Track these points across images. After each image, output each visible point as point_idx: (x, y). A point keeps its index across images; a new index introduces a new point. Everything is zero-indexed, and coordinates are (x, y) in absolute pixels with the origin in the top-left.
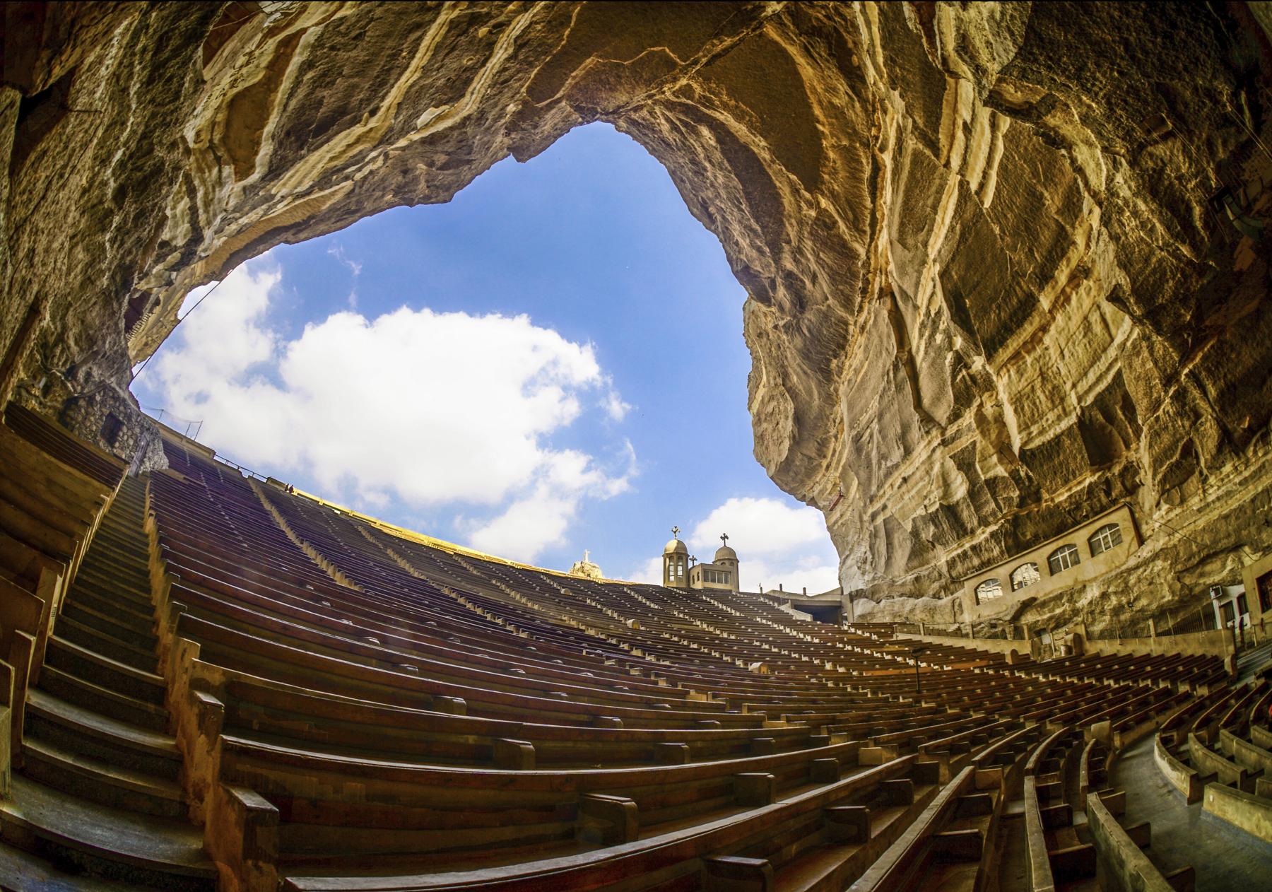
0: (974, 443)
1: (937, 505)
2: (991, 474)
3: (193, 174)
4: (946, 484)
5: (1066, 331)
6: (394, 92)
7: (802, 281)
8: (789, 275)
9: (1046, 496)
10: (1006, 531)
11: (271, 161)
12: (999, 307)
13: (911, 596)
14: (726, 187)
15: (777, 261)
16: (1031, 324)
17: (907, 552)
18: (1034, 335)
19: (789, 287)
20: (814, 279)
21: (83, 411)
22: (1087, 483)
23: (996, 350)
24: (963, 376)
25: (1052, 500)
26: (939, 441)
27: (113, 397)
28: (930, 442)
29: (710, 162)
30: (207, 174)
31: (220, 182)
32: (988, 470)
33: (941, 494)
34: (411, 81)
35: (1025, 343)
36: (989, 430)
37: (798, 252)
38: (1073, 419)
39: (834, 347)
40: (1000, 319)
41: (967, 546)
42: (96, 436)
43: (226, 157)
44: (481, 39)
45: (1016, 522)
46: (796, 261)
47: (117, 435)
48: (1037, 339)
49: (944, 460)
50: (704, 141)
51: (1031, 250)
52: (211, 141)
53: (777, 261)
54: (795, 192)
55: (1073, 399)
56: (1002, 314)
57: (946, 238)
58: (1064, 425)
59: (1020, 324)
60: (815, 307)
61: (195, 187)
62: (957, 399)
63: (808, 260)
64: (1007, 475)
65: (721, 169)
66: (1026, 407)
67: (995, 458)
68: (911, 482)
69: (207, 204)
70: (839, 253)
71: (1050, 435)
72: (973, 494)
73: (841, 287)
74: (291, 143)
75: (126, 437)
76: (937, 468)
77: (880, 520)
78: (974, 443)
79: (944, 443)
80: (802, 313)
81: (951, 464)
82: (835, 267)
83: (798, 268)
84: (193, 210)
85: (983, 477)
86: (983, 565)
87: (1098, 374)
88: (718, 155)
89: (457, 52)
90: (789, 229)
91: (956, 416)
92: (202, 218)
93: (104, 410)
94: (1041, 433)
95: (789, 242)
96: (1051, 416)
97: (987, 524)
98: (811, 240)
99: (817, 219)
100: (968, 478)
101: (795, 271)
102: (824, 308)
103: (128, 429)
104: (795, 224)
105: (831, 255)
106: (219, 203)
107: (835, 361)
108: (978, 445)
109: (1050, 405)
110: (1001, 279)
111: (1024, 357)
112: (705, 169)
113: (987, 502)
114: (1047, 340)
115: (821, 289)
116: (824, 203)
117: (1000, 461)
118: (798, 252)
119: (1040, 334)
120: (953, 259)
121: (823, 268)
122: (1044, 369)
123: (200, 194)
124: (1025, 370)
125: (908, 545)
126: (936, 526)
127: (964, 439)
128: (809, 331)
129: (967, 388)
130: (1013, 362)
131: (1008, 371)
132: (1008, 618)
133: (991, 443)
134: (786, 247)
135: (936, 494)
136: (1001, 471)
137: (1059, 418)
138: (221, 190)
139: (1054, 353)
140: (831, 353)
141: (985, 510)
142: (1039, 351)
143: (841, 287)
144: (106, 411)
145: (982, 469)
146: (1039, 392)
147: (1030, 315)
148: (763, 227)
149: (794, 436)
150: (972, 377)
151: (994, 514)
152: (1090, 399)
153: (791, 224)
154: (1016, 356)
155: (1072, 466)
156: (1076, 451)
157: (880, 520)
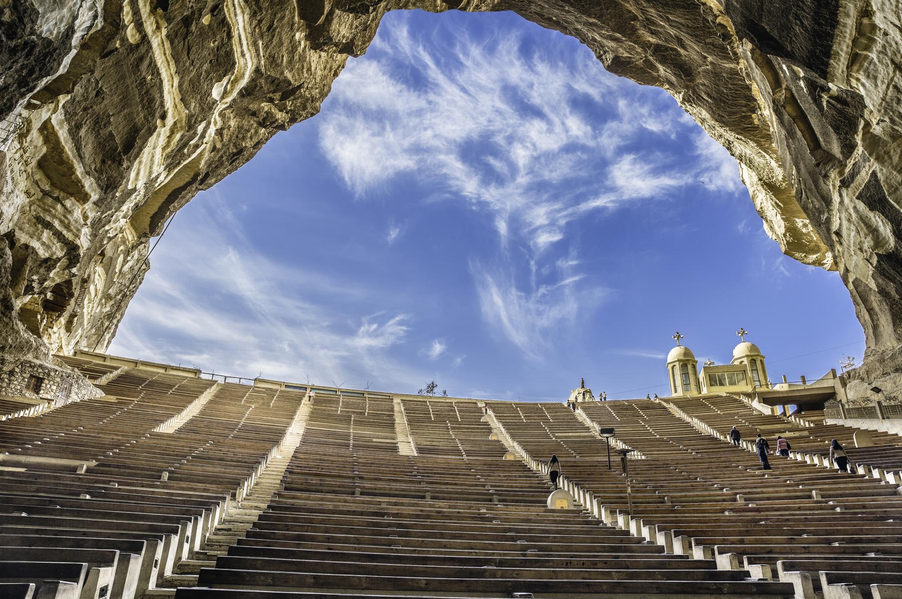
0: (874, 174)
3: (42, 215)
4: (873, 231)
6: (167, 96)
7: (673, 49)
8: (658, 50)
11: (99, 185)
12: (797, 17)
15: (638, 40)
16: (848, 15)
18: (859, 28)
19: (663, 61)
21: (6, 380)
23: (827, 65)
24: (828, 101)
26: (838, 184)
27: (31, 366)
30: (53, 211)
31: (68, 211)
33: (872, 243)
34: (176, 83)
35: (855, 41)
36: (887, 153)
37: (649, 23)
40: (806, 30)
42: (21, 391)
43: (62, 194)
44: (209, 25)
46: (653, 33)
47: (40, 386)
48: (867, 30)
52: (42, 191)
53: (638, 40)
56: (806, 22)
59: (834, 22)
60: (700, 69)
61: (49, 222)
62: (837, 129)
63: (663, 27)
68: (844, 233)
69: (67, 227)
70: (684, 7)
73: (708, 40)
74: (110, 166)
75: (48, 386)
76: (854, 215)
78: (874, 174)
80: (692, 80)
81: (861, 206)
82: (690, 24)
83: (660, 39)
84: (59, 235)
89: (194, 48)
91: (849, 148)
92: (69, 236)
93: (24, 375)
95: (635, 18)
98: (651, 7)
100: (886, 217)
103: (49, 381)
105: (679, 12)
106: (76, 222)
107: (754, 116)
108: (879, 175)
111: (866, 57)
115: (692, 51)
118: (649, 23)
119: (866, 21)
121: (679, 28)
123: (56, 224)
124: (876, 71)
125: (885, 307)
127: (863, 173)
129: (840, 112)
130: (855, 68)
131: (858, 80)
133: (895, 168)
134: (638, 25)
135: (868, 243)
138: (72, 215)
140: (744, 109)
142: (879, 39)
143: (708, 40)
144: (27, 375)
150: (837, 99)
154: (854, 59)
157: (851, 286)
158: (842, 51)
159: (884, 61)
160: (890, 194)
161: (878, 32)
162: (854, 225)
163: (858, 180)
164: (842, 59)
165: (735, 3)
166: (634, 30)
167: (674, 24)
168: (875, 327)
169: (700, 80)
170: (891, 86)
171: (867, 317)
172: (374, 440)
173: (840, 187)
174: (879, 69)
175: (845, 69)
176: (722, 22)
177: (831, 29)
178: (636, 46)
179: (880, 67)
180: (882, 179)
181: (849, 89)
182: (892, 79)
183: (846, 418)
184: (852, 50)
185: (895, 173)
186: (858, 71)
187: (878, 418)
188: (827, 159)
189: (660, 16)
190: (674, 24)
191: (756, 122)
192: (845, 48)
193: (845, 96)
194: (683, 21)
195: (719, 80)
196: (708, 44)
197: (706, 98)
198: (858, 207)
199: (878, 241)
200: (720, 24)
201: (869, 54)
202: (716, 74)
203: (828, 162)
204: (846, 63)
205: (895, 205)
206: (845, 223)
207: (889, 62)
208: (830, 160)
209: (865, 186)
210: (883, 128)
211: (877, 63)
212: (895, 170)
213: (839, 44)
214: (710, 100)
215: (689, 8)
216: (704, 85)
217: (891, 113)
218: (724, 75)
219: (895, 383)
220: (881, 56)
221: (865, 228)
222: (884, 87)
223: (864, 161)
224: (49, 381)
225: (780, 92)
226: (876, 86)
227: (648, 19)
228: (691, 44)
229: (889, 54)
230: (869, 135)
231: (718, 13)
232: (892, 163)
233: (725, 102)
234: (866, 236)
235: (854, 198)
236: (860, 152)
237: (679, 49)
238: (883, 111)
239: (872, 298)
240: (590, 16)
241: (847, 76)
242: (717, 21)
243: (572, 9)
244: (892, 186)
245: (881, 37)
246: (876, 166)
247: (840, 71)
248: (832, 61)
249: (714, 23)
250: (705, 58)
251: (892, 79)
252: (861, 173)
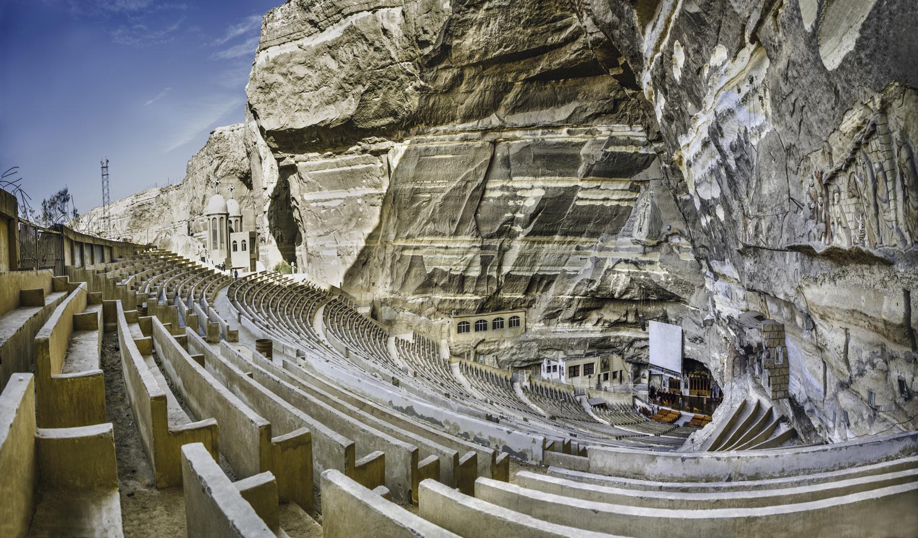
1: (459, 273)
17: (419, 283)
22: (518, 297)
38: (531, 275)
55: (537, 268)
58: (527, 274)
71: (520, 274)
79: (482, 248)
81: (478, 259)
94: (518, 271)
113: (483, 285)
114: (545, 246)
126: (450, 281)
136: (495, 274)
137: (527, 271)
146: (529, 258)
151: (483, 292)
152: (541, 273)
154: (534, 242)
155: (518, 288)
156: (523, 285)
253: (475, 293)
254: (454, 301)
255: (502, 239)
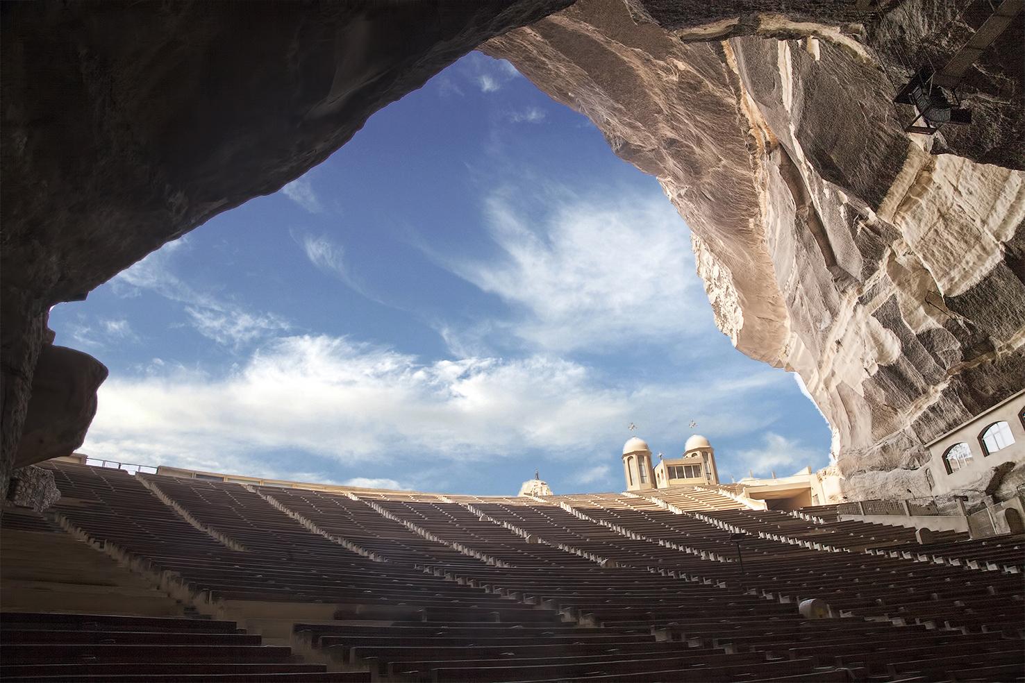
0: (894, 297)
1: (877, 368)
2: (923, 328)
4: (879, 345)
5: (952, 166)
7: (688, 146)
8: (672, 142)
9: (998, 343)
10: (959, 388)
13: (883, 469)
14: (572, 75)
17: (869, 420)
18: (918, 178)
19: (676, 156)
20: (699, 142)
23: (881, 201)
24: (863, 228)
25: (1009, 347)
26: (857, 300)
28: (849, 302)
29: (545, 56)
32: (918, 325)
33: (877, 356)
38: (998, 257)
39: (745, 207)
40: (872, 168)
41: (925, 407)
45: (966, 375)
48: (923, 181)
49: (866, 320)
50: (531, 39)
51: (878, 94)
54: (647, 62)
55: (989, 238)
56: (874, 164)
57: (793, 95)
58: (990, 264)
59: (898, 168)
60: (711, 170)
62: (864, 253)
64: (941, 326)
65: (559, 61)
66: (937, 253)
67: (922, 310)
68: (845, 343)
71: (976, 278)
72: (907, 351)
73: (729, 146)
77: (833, 388)
78: (894, 297)
79: (862, 301)
81: (875, 323)
85: (913, 332)
86: (950, 427)
87: (1008, 205)
88: (549, 49)
90: (656, 99)
91: (870, 270)
95: (660, 112)
96: (971, 257)
97: (936, 383)
99: (680, 82)
101: (678, 138)
102: (721, 170)
104: (659, 92)
105: (708, 115)
107: (751, 220)
109: (964, 246)
110: (861, 128)
111: (916, 202)
112: (544, 63)
113: (925, 358)
114: (937, 177)
115: (707, 152)
116: (682, 66)
117: (929, 312)
118: (672, 119)
119: (926, 174)
120: (804, 117)
122: (944, 210)
125: (867, 411)
127: (882, 294)
128: (713, 196)
129: (871, 239)
130: (904, 208)
132: (984, 488)
135: (872, 355)
136: (932, 323)
139: (948, 190)
140: (744, 213)
141: (927, 367)
142: (931, 190)
143: (729, 146)
145: (911, 325)
146: (946, 235)
147: (905, 157)
148: (626, 105)
149: (743, 301)
150: (872, 228)
152: (1010, 234)
153: (655, 94)
154: (906, 202)
157: (833, 388)
158: (897, 192)
159: (931, 209)
160: (905, 316)
161: (932, 184)
162: (861, 337)
163: (876, 299)
164: (895, 199)
165: (809, 132)
166: (656, 122)
167: (700, 125)
168: (852, 428)
169: (707, 179)
170: (933, 229)
171: (844, 417)
172: (432, 548)
173: (857, 303)
174: (925, 213)
175: (895, 208)
176: (753, 134)
177: (894, 174)
178: (652, 137)
179: (926, 212)
180: (901, 302)
181: (892, 224)
182: (935, 224)
183: (865, 515)
184: (907, 193)
185: (913, 299)
186: (906, 211)
187: (861, 514)
188: (843, 277)
189: (689, 115)
190: (700, 125)
191: (751, 226)
192: (900, 191)
193: (880, 226)
194: (710, 124)
195: (727, 183)
196: (729, 149)
197: (711, 198)
198: (870, 323)
199: (882, 353)
200: (750, 135)
201: (920, 200)
202: (724, 177)
203: (845, 279)
204: (898, 203)
205: (908, 326)
206: (851, 334)
207: (936, 210)
208: (847, 278)
209: (882, 306)
210: (908, 260)
211: (925, 208)
212: (914, 296)
213: (897, 186)
214: (713, 199)
215: (719, 114)
216: (709, 184)
217: (926, 251)
218: (733, 179)
219: (873, 480)
220: (930, 204)
221: (872, 342)
222: (927, 229)
223: (886, 284)
224: (25, 482)
225: (804, 208)
226: (919, 226)
227: (673, 115)
228: (710, 145)
229: (938, 204)
230: (893, 263)
231: (752, 126)
232: (910, 291)
233: (727, 204)
234: (872, 348)
235: (870, 315)
236: (882, 276)
237: (694, 147)
238: (919, 247)
239: (854, 402)
240: (618, 101)
241: (895, 213)
242: (749, 133)
243: (602, 92)
244: (909, 310)
245: (934, 189)
246: (897, 291)
247: (890, 209)
248: (885, 199)
249: (745, 133)
250: (720, 160)
251: (935, 224)
252: (880, 295)
253: (931, 380)
254: (926, 416)
255: (887, 253)
